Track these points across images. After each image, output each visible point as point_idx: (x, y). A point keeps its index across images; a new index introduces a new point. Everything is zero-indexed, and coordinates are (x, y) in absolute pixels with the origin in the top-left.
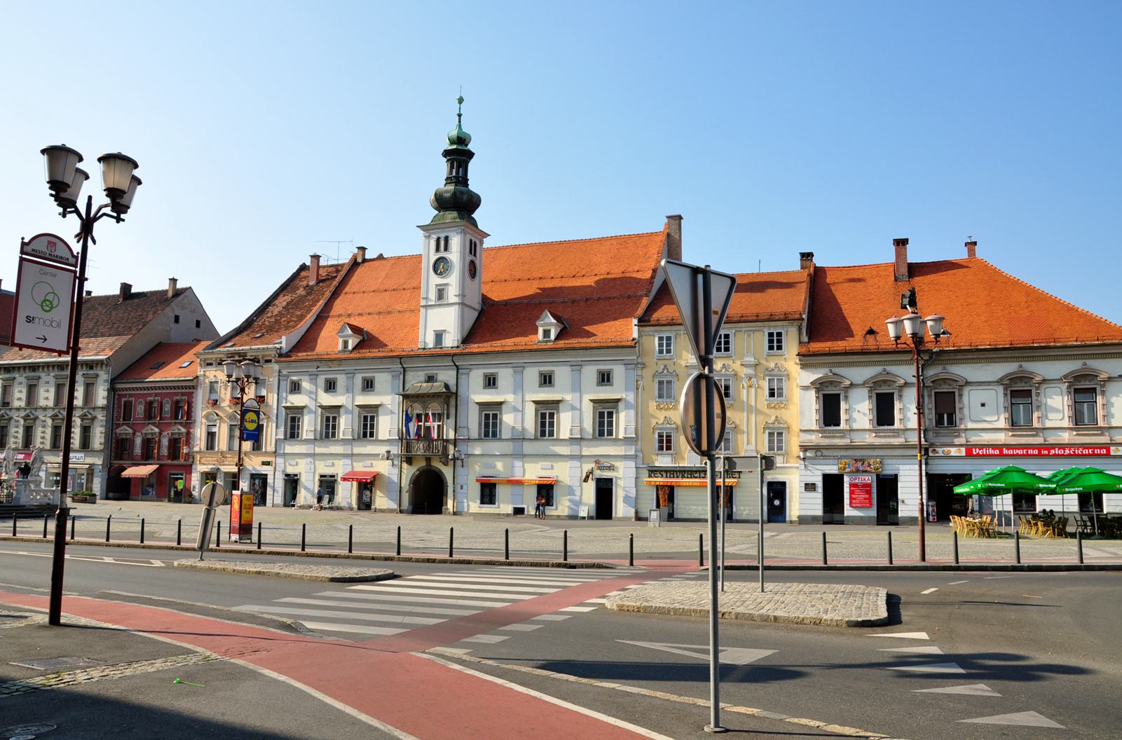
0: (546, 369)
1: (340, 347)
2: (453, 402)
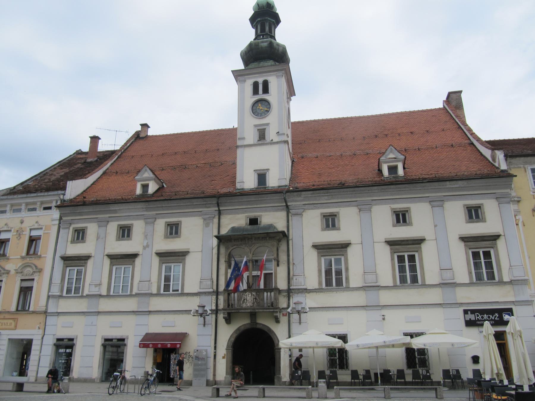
0: (400, 206)
1: (139, 191)
2: (283, 247)
